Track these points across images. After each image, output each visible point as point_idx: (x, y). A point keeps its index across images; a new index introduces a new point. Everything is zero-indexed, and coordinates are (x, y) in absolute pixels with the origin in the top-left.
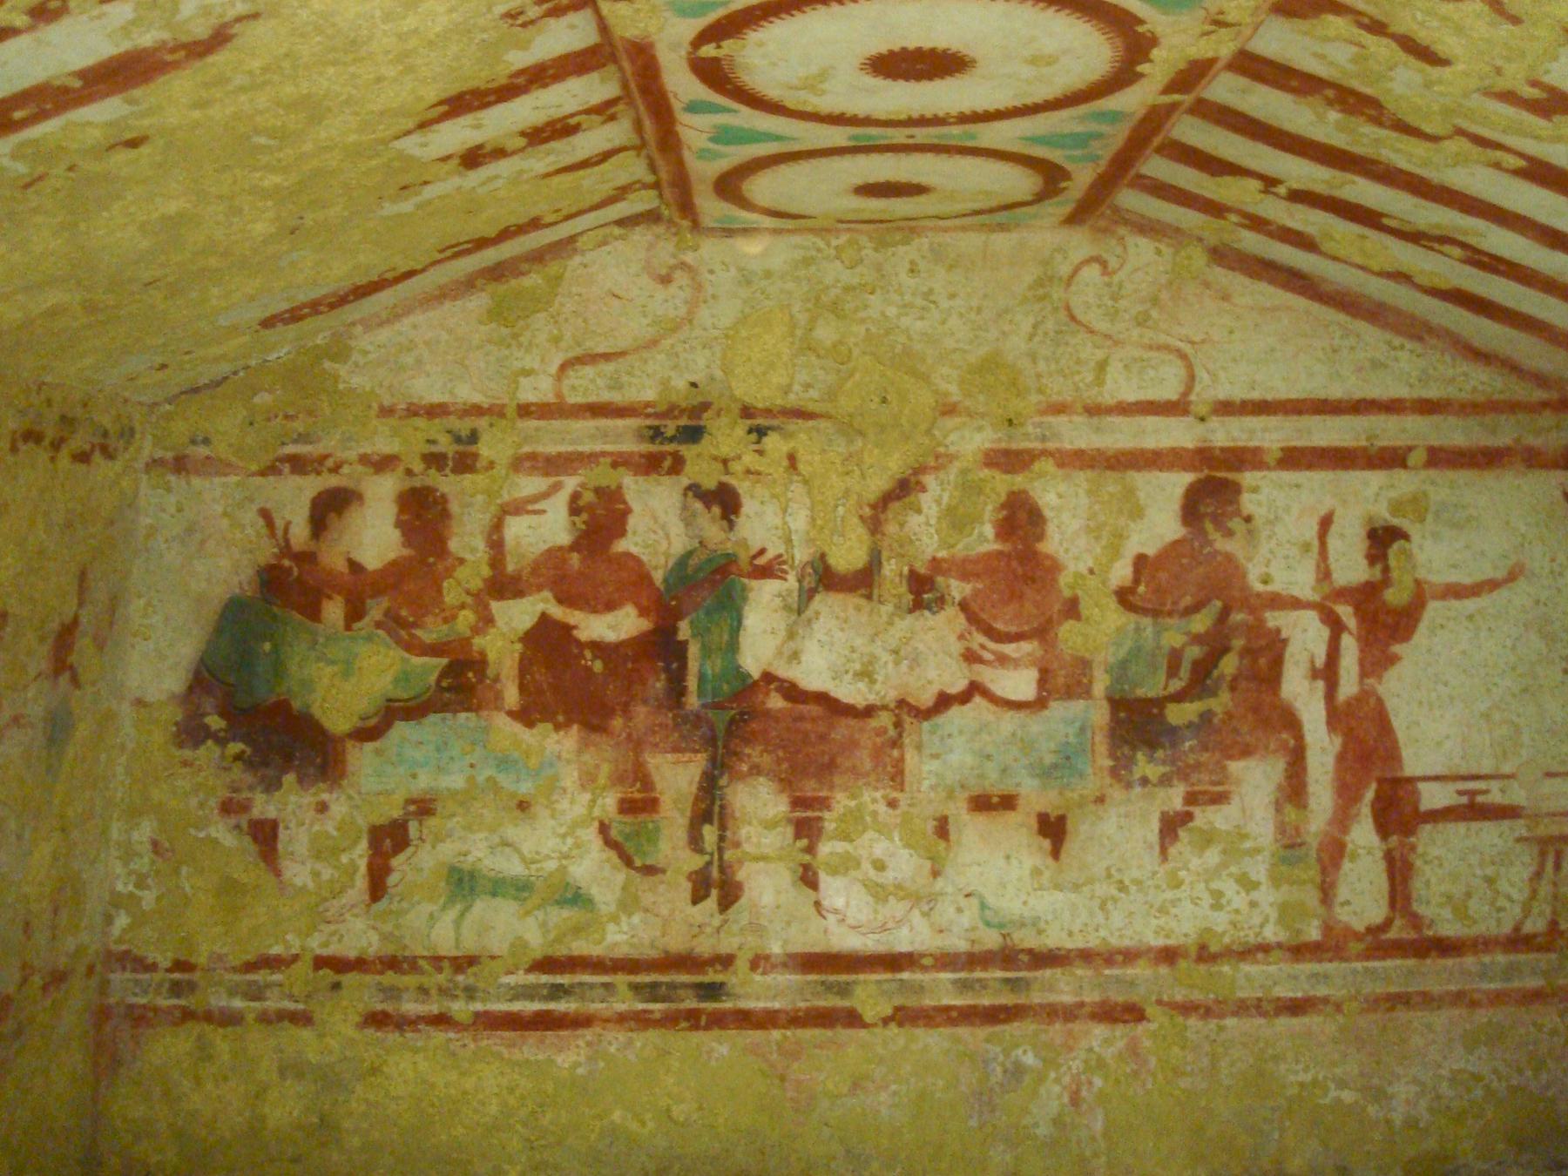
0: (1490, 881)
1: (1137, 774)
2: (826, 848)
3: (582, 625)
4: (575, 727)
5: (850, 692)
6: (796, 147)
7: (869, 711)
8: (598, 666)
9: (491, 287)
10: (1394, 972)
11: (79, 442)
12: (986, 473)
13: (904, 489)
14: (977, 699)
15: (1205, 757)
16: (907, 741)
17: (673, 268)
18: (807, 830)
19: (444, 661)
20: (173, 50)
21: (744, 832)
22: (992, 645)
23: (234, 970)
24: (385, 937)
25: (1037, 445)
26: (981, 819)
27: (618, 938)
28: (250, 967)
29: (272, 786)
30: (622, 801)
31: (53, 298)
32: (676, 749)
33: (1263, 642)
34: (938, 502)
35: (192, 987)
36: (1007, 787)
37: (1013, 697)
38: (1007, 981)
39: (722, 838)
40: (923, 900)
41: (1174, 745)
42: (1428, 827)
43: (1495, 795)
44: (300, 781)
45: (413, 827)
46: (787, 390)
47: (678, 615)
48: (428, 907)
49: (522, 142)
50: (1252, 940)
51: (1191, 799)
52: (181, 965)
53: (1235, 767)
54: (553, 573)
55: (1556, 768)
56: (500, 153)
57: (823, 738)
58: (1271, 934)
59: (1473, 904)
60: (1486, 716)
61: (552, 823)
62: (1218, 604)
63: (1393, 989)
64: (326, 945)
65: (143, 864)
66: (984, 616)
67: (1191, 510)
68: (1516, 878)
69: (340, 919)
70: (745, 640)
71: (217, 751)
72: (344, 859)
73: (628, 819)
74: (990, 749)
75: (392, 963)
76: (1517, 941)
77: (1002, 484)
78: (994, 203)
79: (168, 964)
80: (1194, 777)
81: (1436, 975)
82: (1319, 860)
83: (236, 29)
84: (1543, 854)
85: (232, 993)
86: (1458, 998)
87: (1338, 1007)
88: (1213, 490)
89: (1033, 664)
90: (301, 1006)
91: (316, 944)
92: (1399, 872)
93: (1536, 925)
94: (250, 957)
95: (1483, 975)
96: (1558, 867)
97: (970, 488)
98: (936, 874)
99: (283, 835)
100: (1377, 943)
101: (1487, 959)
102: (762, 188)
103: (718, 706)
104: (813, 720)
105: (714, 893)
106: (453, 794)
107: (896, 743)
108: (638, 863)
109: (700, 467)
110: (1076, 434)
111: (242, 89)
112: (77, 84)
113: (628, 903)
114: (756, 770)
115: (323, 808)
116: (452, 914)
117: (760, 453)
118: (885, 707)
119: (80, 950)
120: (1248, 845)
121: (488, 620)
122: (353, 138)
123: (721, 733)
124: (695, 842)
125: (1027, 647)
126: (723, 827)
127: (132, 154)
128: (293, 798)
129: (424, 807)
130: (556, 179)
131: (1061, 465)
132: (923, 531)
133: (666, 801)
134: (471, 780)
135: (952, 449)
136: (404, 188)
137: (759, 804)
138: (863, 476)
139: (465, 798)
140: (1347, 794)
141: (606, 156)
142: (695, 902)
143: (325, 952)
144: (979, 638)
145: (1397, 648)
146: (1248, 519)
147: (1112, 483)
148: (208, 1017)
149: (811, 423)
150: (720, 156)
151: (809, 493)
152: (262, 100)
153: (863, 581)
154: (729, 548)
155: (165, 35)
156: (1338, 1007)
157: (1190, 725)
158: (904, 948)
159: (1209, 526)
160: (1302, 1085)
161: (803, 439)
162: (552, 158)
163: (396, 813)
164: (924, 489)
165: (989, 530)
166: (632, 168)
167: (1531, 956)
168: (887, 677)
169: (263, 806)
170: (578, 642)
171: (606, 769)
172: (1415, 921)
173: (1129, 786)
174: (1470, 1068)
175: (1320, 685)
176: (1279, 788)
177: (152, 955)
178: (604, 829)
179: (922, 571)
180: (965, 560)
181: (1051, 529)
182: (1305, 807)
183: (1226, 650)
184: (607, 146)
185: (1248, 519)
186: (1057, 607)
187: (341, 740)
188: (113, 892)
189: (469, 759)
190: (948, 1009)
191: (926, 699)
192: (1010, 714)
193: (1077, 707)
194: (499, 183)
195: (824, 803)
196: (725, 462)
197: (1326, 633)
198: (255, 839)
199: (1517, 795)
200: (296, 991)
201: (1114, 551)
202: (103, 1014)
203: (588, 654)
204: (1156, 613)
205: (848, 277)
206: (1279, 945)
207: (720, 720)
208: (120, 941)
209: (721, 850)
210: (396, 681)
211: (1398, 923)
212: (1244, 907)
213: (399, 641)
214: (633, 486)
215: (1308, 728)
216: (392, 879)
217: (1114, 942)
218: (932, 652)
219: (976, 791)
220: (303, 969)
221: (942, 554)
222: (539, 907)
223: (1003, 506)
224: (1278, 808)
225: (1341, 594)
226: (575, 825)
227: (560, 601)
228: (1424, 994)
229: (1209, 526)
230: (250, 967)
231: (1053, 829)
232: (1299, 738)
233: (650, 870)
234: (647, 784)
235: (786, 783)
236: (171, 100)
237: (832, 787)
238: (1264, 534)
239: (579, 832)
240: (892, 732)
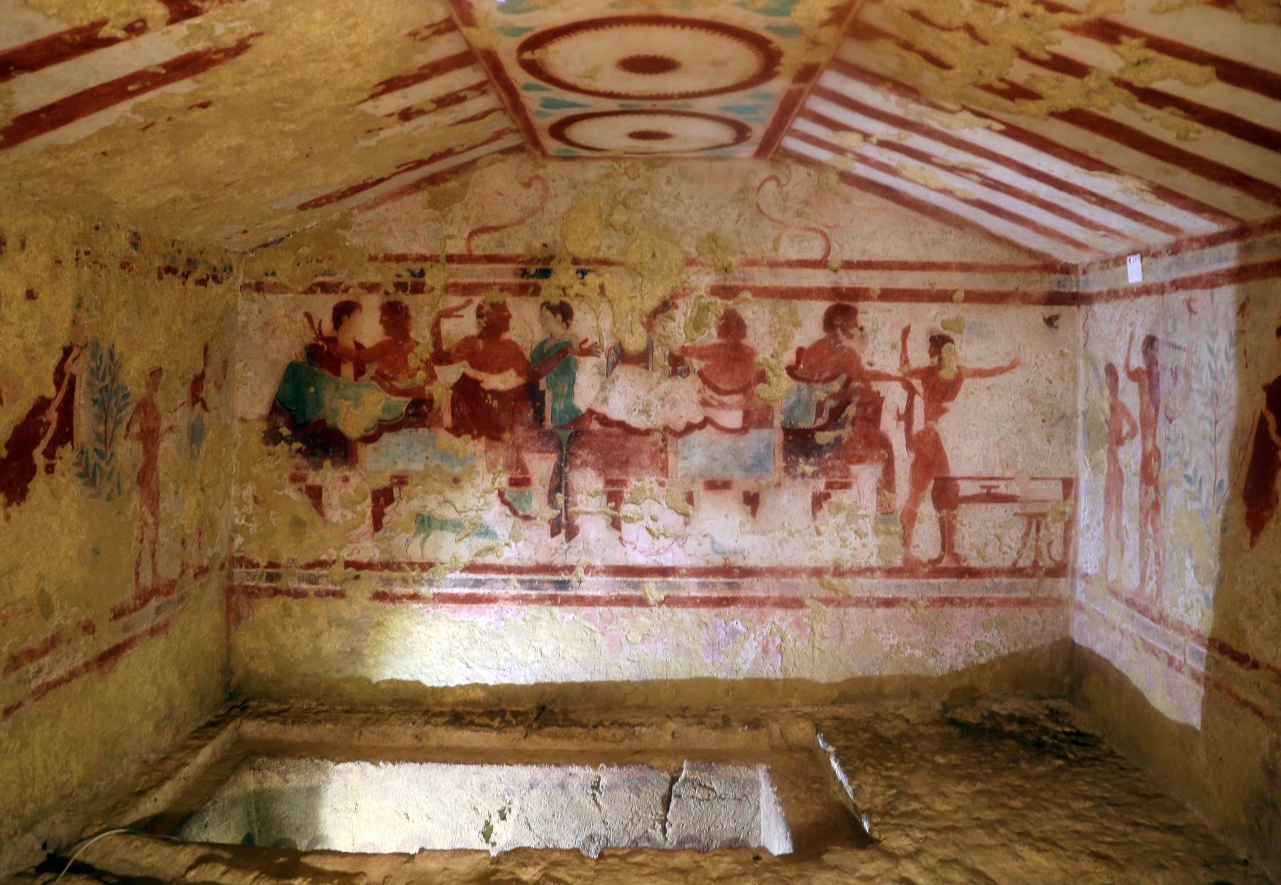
0: (999, 538)
1: (800, 471)
2: (627, 509)
3: (486, 380)
4: (483, 438)
5: (636, 421)
6: (590, 111)
7: (647, 432)
8: (495, 403)
9: (430, 188)
10: (945, 586)
11: (200, 273)
12: (714, 299)
13: (666, 306)
14: (709, 427)
15: (837, 463)
16: (669, 449)
17: (531, 179)
18: (614, 497)
19: (410, 399)
20: (217, 52)
21: (579, 498)
22: (716, 396)
23: (301, 567)
24: (382, 551)
25: (740, 283)
26: (711, 495)
27: (509, 555)
28: (310, 566)
29: (318, 467)
30: (511, 479)
31: (173, 192)
32: (539, 451)
33: (869, 399)
34: (685, 315)
35: (278, 576)
36: (727, 476)
37: (729, 426)
38: (728, 584)
39: (566, 501)
40: (679, 538)
41: (819, 456)
42: (964, 505)
43: (1002, 489)
44: (333, 465)
45: (396, 492)
46: (598, 249)
47: (539, 376)
48: (404, 536)
49: (433, 106)
50: (863, 565)
51: (830, 485)
52: (271, 565)
53: (854, 468)
54: (467, 350)
55: (1036, 475)
56: (421, 112)
57: (623, 447)
58: (874, 562)
59: (989, 549)
60: (998, 444)
61: (472, 490)
62: (844, 376)
63: (943, 595)
64: (350, 555)
65: (249, 508)
66: (712, 380)
67: (829, 322)
68: (1014, 536)
69: (358, 541)
70: (577, 390)
71: (287, 447)
72: (359, 508)
73: (515, 489)
74: (717, 455)
75: (387, 565)
76: (1015, 571)
77: (721, 304)
78: (711, 144)
79: (265, 564)
80: (831, 473)
81: (967, 588)
82: (902, 522)
83: (251, 41)
84: (1030, 524)
85: (301, 579)
86: (980, 601)
87: (913, 604)
88: (842, 311)
89: (740, 407)
90: (338, 588)
91: (345, 555)
92: (947, 531)
93: (1025, 562)
94: (311, 561)
95: (996, 588)
96: (1038, 530)
97: (703, 309)
98: (686, 524)
99: (324, 494)
100: (935, 569)
101: (997, 580)
102: (579, 132)
103: (563, 427)
104: (617, 437)
105: (563, 531)
106: (417, 473)
107: (662, 450)
108: (521, 513)
109: (550, 291)
110: (763, 278)
111: (262, 76)
112: (163, 71)
113: (515, 537)
114: (585, 464)
115: (346, 479)
116: (418, 540)
117: (584, 284)
118: (657, 430)
119: (215, 556)
120: (861, 512)
121: (433, 377)
122: (333, 103)
123: (565, 443)
124: (552, 503)
125: (736, 398)
126: (567, 494)
127: (204, 111)
128: (329, 474)
129: (401, 480)
130: (458, 127)
131: (754, 295)
132: (677, 330)
133: (535, 481)
134: (426, 466)
135: (693, 285)
136: (369, 131)
137: (587, 483)
138: (642, 298)
139: (425, 476)
140: (917, 486)
141: (485, 114)
142: (553, 536)
143: (350, 559)
144: (709, 393)
145: (946, 404)
146: (862, 329)
147: (783, 308)
148: (288, 593)
149: (612, 268)
150: (549, 115)
151: (612, 308)
152: (275, 81)
153: (642, 359)
154: (567, 338)
155: (210, 44)
156: (913, 604)
157: (828, 444)
158: (669, 564)
159: (840, 332)
160: (891, 646)
161: (608, 277)
162: (452, 115)
163: (386, 483)
164: (677, 307)
165: (714, 332)
166: (501, 121)
167: (1023, 580)
168: (658, 413)
169: (314, 478)
170: (484, 390)
171: (501, 460)
172: (956, 557)
173: (794, 477)
174: (987, 640)
175: (903, 423)
176: (879, 481)
177: (256, 559)
178: (501, 494)
179: (677, 353)
180: (701, 348)
181: (749, 332)
182: (894, 492)
183: (849, 403)
184: (485, 109)
185: (862, 329)
186: (753, 376)
187: (355, 442)
188: (233, 524)
189: (425, 454)
190: (695, 598)
191: (680, 426)
192: (727, 436)
193: (765, 432)
194: (423, 130)
195: (623, 483)
196: (564, 290)
197: (905, 394)
198: (310, 496)
199: (1014, 489)
200: (336, 579)
201: (784, 345)
202: (230, 591)
203: (489, 396)
204: (808, 381)
205: (633, 185)
206: (879, 568)
207: (564, 435)
208: (239, 551)
209: (566, 507)
210: (383, 410)
211: (945, 559)
212: (859, 548)
213: (384, 388)
214: (512, 303)
215: (895, 447)
216: (385, 520)
217: (786, 564)
218: (682, 399)
219: (709, 478)
220: (339, 568)
221: (688, 344)
222: (467, 535)
223: (722, 318)
224: (879, 491)
225: (914, 373)
226: (486, 492)
227: (473, 366)
228: (961, 599)
229: (840, 332)
230: (310, 566)
231: (752, 501)
232: (891, 453)
233: (527, 518)
234: (524, 470)
235: (602, 470)
236: (221, 80)
237: (627, 475)
238: (870, 338)
239: (487, 496)
240: (661, 443)
